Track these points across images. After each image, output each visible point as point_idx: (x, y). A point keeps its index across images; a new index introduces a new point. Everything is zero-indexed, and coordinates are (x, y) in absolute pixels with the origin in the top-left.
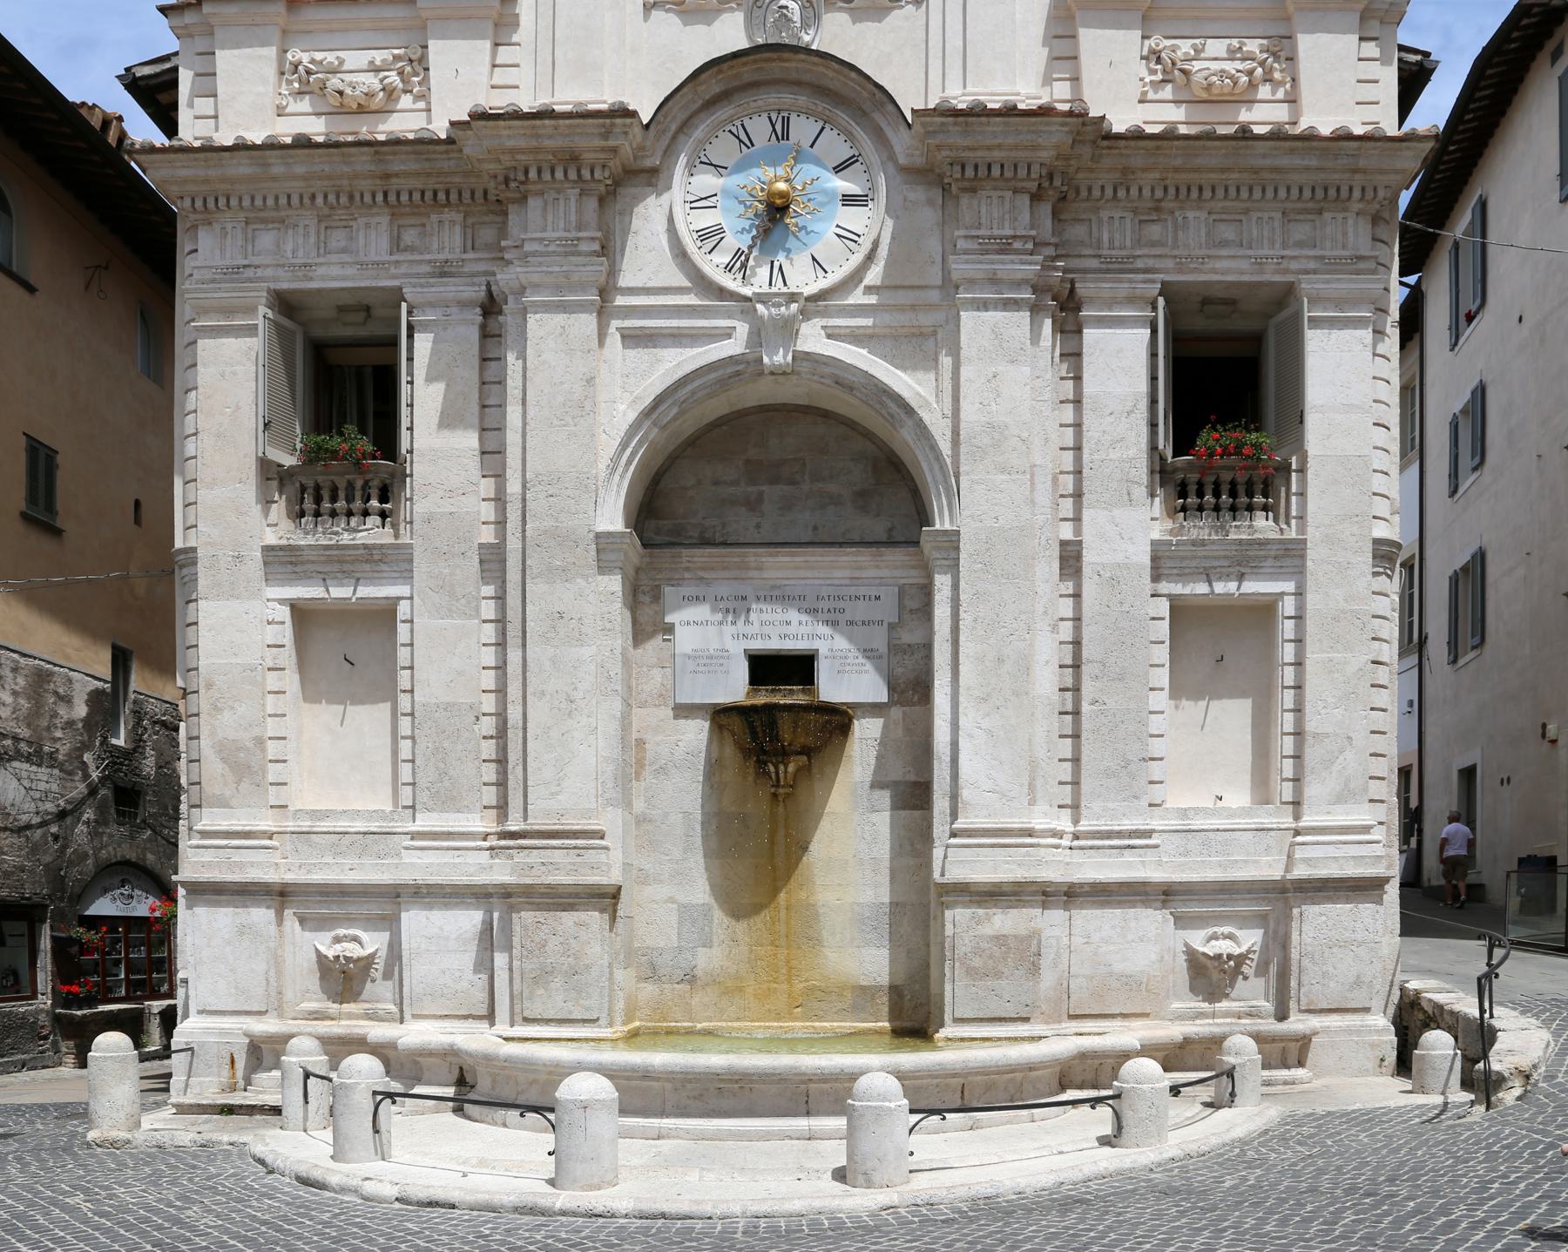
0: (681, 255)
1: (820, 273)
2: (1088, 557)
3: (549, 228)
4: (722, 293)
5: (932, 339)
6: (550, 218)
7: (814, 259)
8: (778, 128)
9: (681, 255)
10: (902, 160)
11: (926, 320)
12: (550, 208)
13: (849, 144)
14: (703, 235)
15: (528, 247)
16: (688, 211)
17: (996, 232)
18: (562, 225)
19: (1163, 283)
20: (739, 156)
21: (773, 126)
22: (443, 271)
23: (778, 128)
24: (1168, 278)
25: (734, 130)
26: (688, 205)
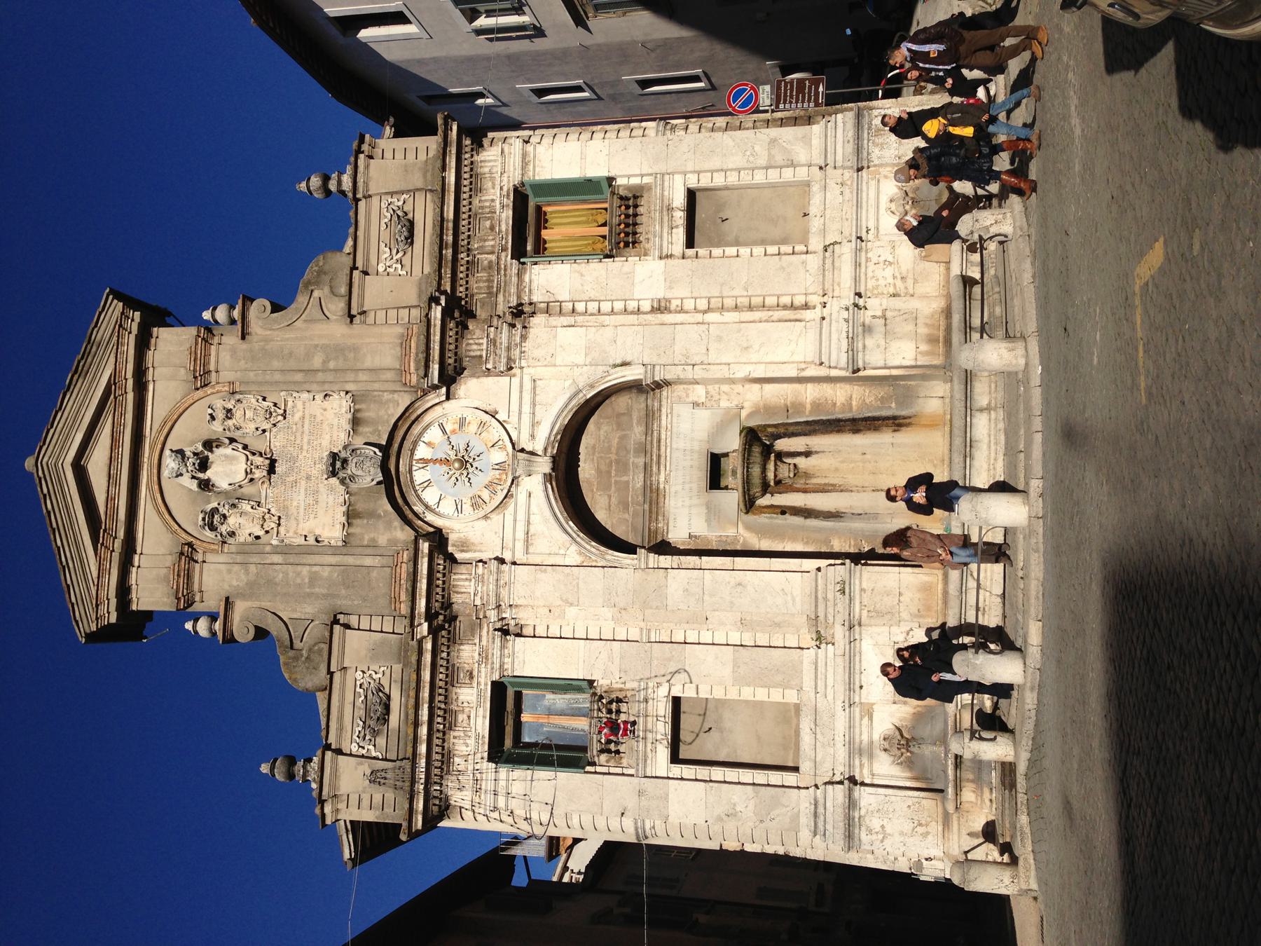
1: (500, 442)
3: (469, 590)
5: (538, 382)
6: (465, 590)
7: (493, 446)
8: (421, 466)
10: (444, 398)
11: (528, 385)
12: (456, 590)
13: (432, 427)
14: (475, 506)
15: (478, 602)
16: (462, 515)
17: (484, 347)
18: (467, 583)
19: (512, 258)
20: (435, 488)
21: (420, 468)
22: (484, 656)
23: (421, 466)
24: (509, 256)
25: (421, 490)
26: (460, 515)
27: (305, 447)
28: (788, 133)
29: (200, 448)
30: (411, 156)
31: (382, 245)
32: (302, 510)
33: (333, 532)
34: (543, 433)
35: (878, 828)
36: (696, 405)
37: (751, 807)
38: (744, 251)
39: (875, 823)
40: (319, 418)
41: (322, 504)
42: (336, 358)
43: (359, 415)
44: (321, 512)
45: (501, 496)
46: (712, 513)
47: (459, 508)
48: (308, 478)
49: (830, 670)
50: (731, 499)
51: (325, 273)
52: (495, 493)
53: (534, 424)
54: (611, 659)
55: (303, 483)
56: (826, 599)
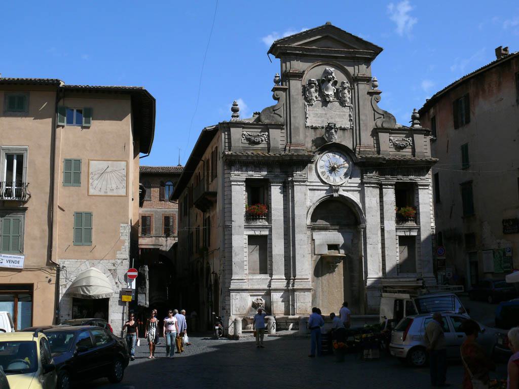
0: (319, 176)
2: (385, 229)
4: (326, 183)
9: (319, 176)
14: (322, 173)
27: (335, 113)
28: (431, 266)
29: (335, 79)
30: (425, 147)
31: (398, 138)
32: (316, 112)
33: (308, 124)
34: (345, 194)
35: (237, 297)
36: (352, 240)
37: (238, 260)
38: (398, 254)
39: (238, 297)
40: (344, 117)
41: (318, 119)
42: (363, 124)
43: (346, 131)
44: (315, 119)
45: (326, 181)
46: (321, 245)
47: (322, 167)
48: (326, 114)
49: (280, 283)
50: (326, 251)
51: (389, 119)
52: (326, 179)
53: (347, 191)
54: (278, 216)
55: (324, 113)
56: (302, 282)
